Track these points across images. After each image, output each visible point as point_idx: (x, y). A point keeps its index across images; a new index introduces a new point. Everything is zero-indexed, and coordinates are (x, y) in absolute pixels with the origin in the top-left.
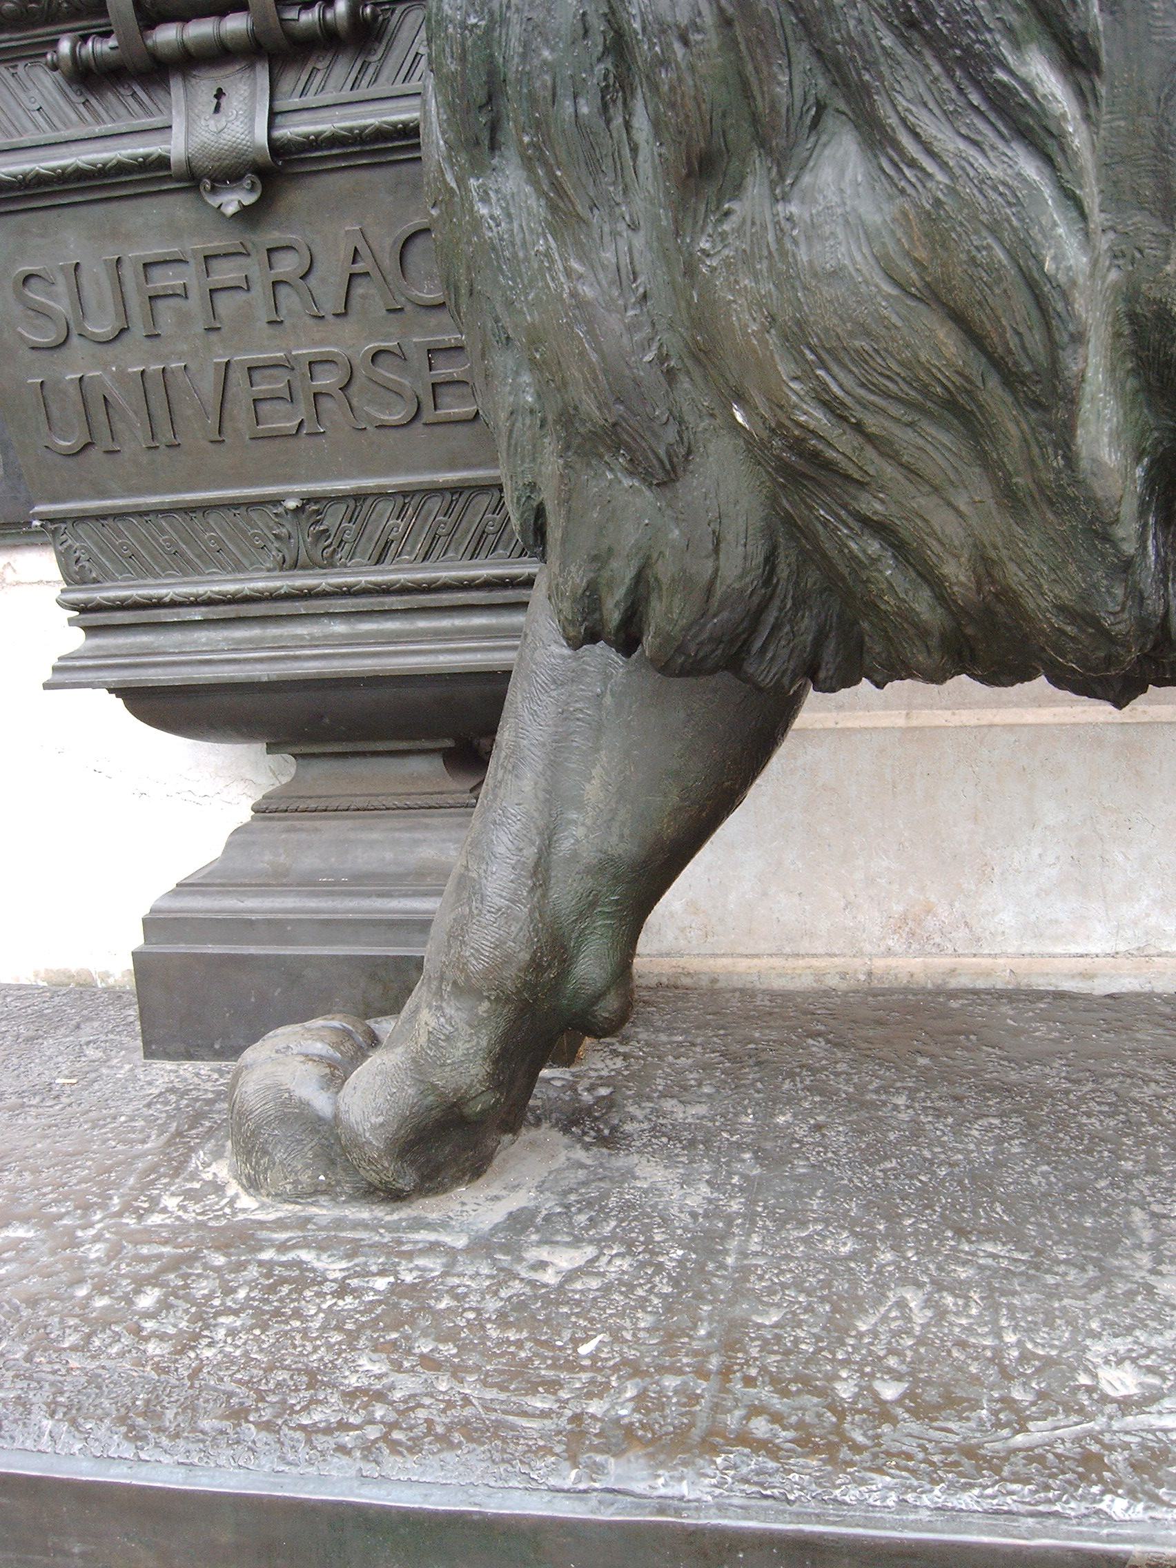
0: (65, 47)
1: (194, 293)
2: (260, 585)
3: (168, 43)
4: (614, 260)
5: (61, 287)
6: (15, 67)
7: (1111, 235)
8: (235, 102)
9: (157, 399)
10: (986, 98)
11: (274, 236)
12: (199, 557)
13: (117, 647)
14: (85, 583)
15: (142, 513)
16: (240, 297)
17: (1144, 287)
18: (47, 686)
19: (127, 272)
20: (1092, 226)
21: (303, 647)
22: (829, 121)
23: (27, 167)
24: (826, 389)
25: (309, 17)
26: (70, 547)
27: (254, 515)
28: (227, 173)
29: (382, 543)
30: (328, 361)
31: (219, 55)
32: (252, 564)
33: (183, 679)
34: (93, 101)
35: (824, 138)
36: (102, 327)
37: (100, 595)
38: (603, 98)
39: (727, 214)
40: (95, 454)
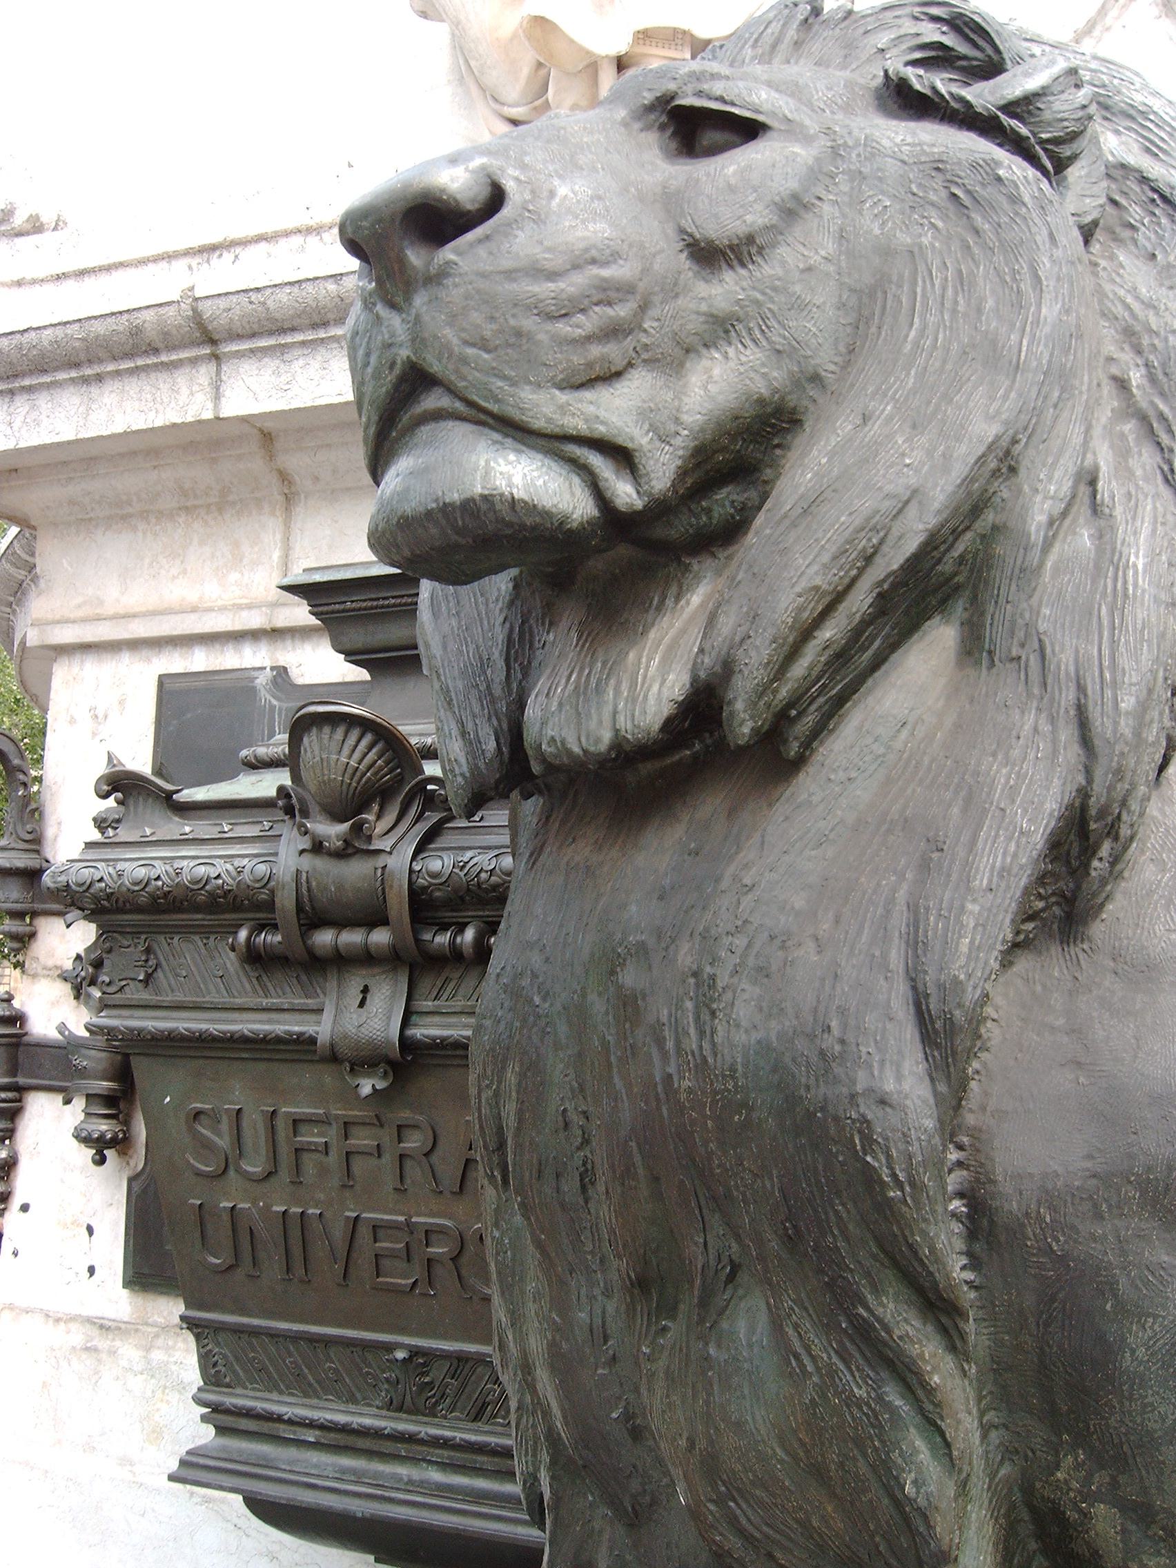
0: (243, 934)
1: (333, 1152)
2: (367, 1421)
3: (324, 946)
4: (588, 1321)
5: (224, 1126)
6: (208, 938)
7: (1002, 1431)
8: (377, 1001)
9: (295, 1233)
10: (851, 1322)
11: (405, 1115)
12: (318, 1382)
13: (240, 1452)
14: (218, 1386)
15: (274, 1335)
16: (373, 1161)
17: (1038, 1485)
18: (172, 1478)
19: (280, 1124)
20: (955, 1453)
21: (398, 1489)
22: (743, 1277)
23: (204, 1026)
24: (736, 1518)
25: (443, 939)
26: (211, 1351)
27: (369, 1356)
28: (365, 1059)
29: (480, 1403)
30: (442, 1230)
31: (367, 958)
32: (364, 1399)
33: (288, 1499)
34: (265, 978)
35: (741, 1292)
36: (254, 1167)
37: (229, 1401)
38: (581, 1180)
39: (665, 1329)
40: (240, 1274)
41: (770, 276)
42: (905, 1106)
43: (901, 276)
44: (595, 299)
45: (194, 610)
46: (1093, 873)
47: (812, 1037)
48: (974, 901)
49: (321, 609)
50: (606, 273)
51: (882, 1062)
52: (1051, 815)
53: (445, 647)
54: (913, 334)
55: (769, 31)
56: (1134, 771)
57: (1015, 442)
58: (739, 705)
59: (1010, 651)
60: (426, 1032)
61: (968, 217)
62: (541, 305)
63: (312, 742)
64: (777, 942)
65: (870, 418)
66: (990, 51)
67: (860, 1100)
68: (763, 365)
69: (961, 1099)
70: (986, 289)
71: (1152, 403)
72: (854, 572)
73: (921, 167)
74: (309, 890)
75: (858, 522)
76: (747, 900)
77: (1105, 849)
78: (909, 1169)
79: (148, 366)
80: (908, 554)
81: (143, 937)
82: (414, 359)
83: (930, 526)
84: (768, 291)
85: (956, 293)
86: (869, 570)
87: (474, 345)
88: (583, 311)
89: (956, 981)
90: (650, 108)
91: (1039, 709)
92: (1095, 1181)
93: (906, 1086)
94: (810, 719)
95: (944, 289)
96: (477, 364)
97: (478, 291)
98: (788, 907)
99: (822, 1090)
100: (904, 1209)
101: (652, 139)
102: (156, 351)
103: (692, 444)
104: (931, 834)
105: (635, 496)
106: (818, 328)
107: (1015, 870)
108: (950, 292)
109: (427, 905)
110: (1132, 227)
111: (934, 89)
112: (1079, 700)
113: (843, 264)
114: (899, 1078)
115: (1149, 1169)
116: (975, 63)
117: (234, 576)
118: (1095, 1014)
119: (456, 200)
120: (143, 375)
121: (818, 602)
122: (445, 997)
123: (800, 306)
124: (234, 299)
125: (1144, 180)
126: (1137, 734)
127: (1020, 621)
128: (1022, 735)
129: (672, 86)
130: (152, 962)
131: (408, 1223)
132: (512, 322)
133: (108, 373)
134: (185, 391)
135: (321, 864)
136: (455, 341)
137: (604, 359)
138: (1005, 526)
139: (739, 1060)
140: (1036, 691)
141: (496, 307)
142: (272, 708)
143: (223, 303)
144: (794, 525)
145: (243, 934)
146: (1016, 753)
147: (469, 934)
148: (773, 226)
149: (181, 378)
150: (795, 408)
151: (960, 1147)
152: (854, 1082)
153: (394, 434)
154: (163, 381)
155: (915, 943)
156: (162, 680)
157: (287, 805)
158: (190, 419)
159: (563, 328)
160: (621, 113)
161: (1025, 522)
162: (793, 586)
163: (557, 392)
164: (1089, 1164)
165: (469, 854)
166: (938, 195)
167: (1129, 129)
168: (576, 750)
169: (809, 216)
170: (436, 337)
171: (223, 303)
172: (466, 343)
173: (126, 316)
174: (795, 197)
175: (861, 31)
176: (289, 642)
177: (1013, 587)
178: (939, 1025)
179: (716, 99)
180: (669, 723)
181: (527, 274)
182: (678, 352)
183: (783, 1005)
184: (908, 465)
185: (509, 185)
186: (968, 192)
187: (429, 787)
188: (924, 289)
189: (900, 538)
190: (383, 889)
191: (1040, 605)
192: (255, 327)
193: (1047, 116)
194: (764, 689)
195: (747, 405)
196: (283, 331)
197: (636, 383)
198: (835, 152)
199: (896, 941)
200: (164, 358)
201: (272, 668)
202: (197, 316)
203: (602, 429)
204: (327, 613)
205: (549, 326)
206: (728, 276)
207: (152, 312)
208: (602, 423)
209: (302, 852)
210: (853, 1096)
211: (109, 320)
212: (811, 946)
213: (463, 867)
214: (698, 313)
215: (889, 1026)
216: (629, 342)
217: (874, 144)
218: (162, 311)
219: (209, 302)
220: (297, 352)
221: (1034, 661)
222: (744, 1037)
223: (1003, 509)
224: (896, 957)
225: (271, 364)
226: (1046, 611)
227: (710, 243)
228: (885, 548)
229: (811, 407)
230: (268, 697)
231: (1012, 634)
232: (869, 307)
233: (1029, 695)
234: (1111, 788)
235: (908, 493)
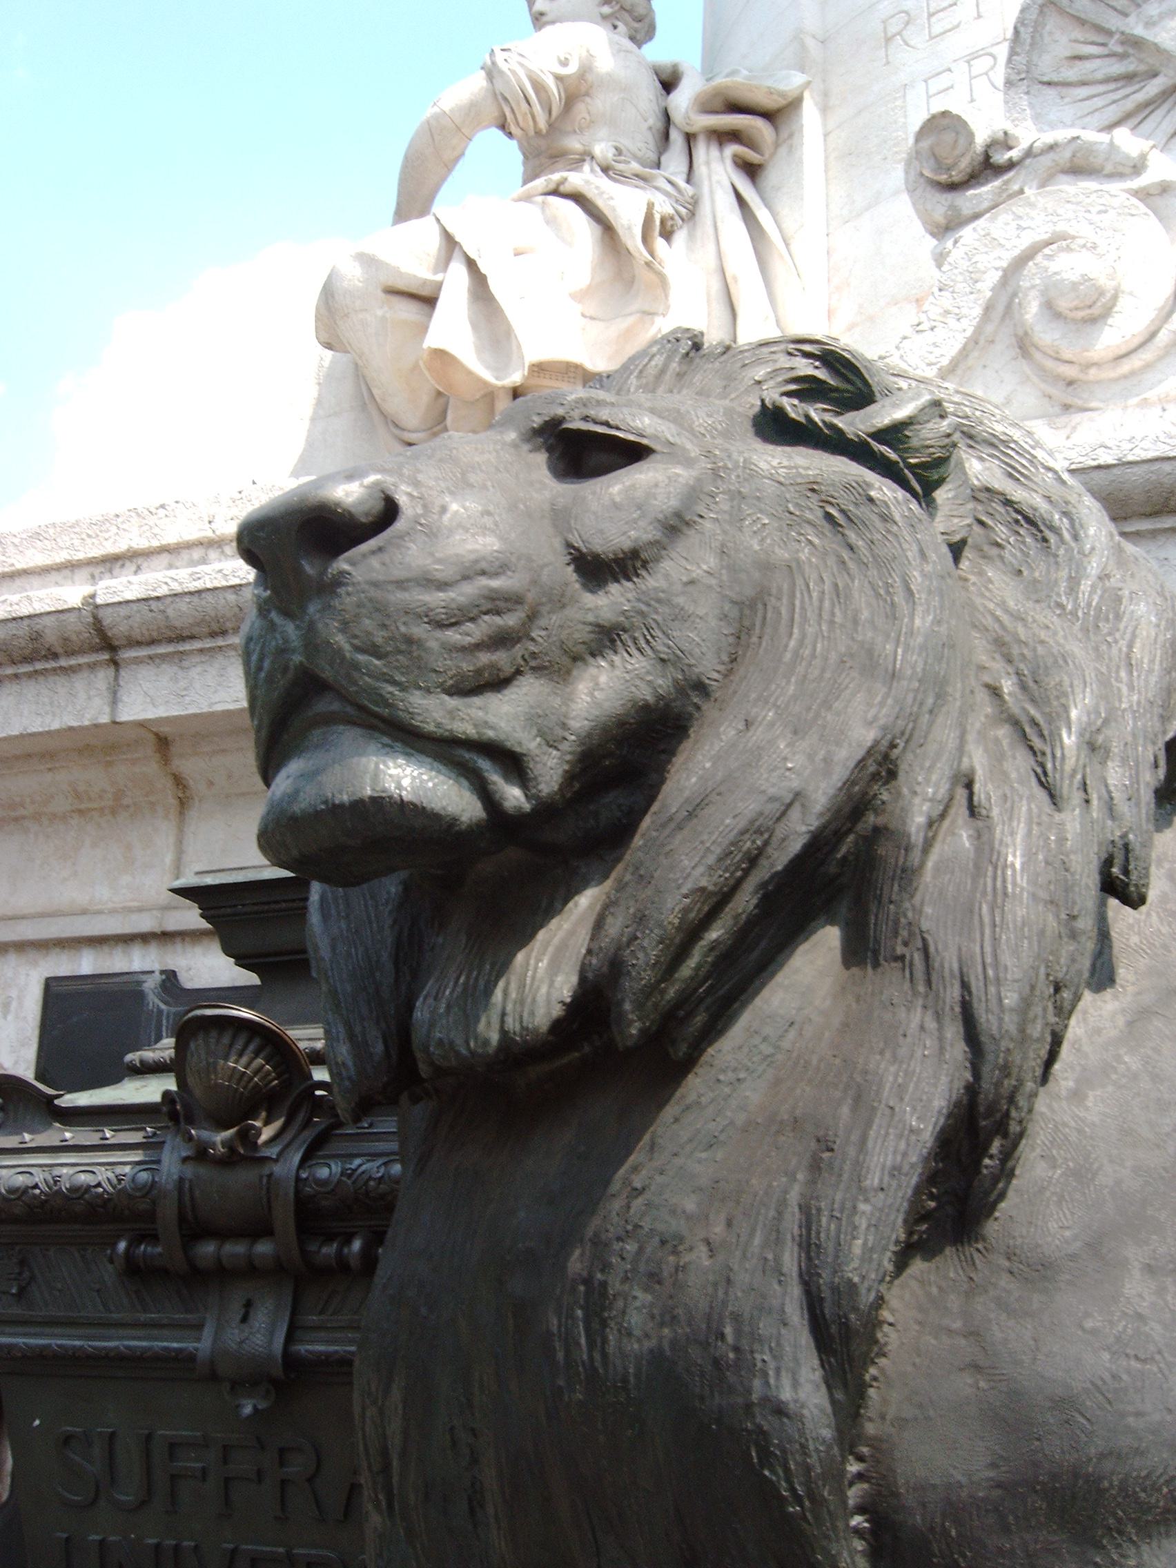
0: (122, 1246)
8: (260, 1319)
25: (330, 1250)
36: (126, 1498)
41: (655, 589)
42: (802, 1416)
43: (780, 589)
44: (484, 609)
45: (84, 912)
46: (985, 1171)
47: (705, 1345)
48: (866, 1200)
49: (212, 912)
50: (495, 583)
51: (778, 1371)
52: (939, 1112)
53: (333, 948)
54: (792, 643)
55: (653, 363)
56: (1021, 1067)
57: (893, 746)
58: (627, 1006)
59: (894, 950)
60: (310, 1347)
63: (197, 1046)
64: (669, 1247)
65: (752, 724)
66: (859, 384)
67: (757, 1410)
68: (648, 673)
69: (859, 1407)
70: (862, 600)
71: (1024, 709)
72: (739, 874)
73: (797, 488)
74: (192, 1198)
75: (742, 823)
76: (638, 1203)
77: (996, 1146)
78: (808, 1483)
79: (46, 670)
80: (791, 855)
81: (18, 1248)
83: (812, 828)
84: (653, 603)
85: (833, 605)
88: (472, 620)
89: (852, 1286)
90: (538, 432)
91: (925, 1007)
92: (998, 1493)
93: (802, 1395)
94: (700, 1019)
95: (821, 601)
96: (368, 670)
97: (371, 600)
99: (717, 1399)
100: (805, 1525)
102: (55, 656)
103: (579, 749)
105: (523, 799)
107: (906, 1168)
108: (827, 604)
109: (316, 1214)
110: (998, 545)
111: (807, 417)
112: (963, 997)
113: (725, 578)
114: (796, 1384)
115: (1054, 1477)
117: (126, 879)
118: (992, 1316)
119: (349, 513)
120: (41, 679)
121: (703, 903)
123: (681, 616)
124: (135, 607)
125: (1008, 503)
126: (1022, 1030)
127: (903, 920)
129: (560, 411)
130: (26, 1274)
131: (289, 1555)
132: (403, 629)
133: (7, 676)
134: (82, 695)
135: (203, 1171)
136: (347, 647)
137: (492, 666)
138: (886, 828)
139: (631, 1371)
140: (921, 988)
142: (160, 1012)
143: (123, 611)
144: (680, 828)
145: (122, 1246)
146: (903, 1052)
147: (357, 1245)
148: (657, 542)
149: (79, 683)
151: (860, 1459)
152: (749, 1391)
153: (286, 737)
154: (61, 685)
155: (809, 1247)
156: (50, 984)
157: (169, 1112)
158: (87, 723)
159: (453, 636)
160: (512, 435)
161: (904, 823)
162: (679, 888)
163: (446, 698)
164: (991, 1474)
165: (357, 1162)
166: (816, 515)
167: (992, 456)
168: (464, 1051)
169: (692, 532)
171: (123, 611)
172: (358, 649)
173: (26, 622)
174: (678, 515)
175: (740, 365)
176: (179, 946)
177: (896, 888)
178: (834, 1329)
180: (557, 1026)
181: (419, 585)
182: (566, 660)
183: (676, 1311)
184: (789, 769)
185: (402, 500)
186: (842, 511)
187: (318, 1093)
188: (802, 602)
189: (784, 840)
190: (269, 1201)
191: (922, 903)
192: (155, 634)
193: (915, 442)
194: (652, 989)
195: (633, 711)
196: (182, 638)
197: (524, 690)
198: (716, 474)
199: (789, 1243)
200: (63, 662)
201: (162, 972)
202: (98, 625)
203: (491, 734)
204: (219, 916)
205: (438, 634)
206: (614, 588)
207: (53, 618)
208: (492, 728)
209: (185, 1160)
210: (749, 1407)
211: (10, 625)
212: (703, 1249)
214: (584, 623)
215: (783, 1331)
216: (518, 650)
218: (62, 617)
219: (110, 610)
220: (196, 659)
221: (918, 958)
222: (636, 1346)
223: (884, 811)
224: (790, 1260)
225: (169, 670)
226: (928, 910)
227: (596, 557)
228: (769, 850)
230: (157, 1001)
231: (896, 933)
232: (750, 617)
233: (915, 993)
234: (998, 1084)
235: (791, 796)
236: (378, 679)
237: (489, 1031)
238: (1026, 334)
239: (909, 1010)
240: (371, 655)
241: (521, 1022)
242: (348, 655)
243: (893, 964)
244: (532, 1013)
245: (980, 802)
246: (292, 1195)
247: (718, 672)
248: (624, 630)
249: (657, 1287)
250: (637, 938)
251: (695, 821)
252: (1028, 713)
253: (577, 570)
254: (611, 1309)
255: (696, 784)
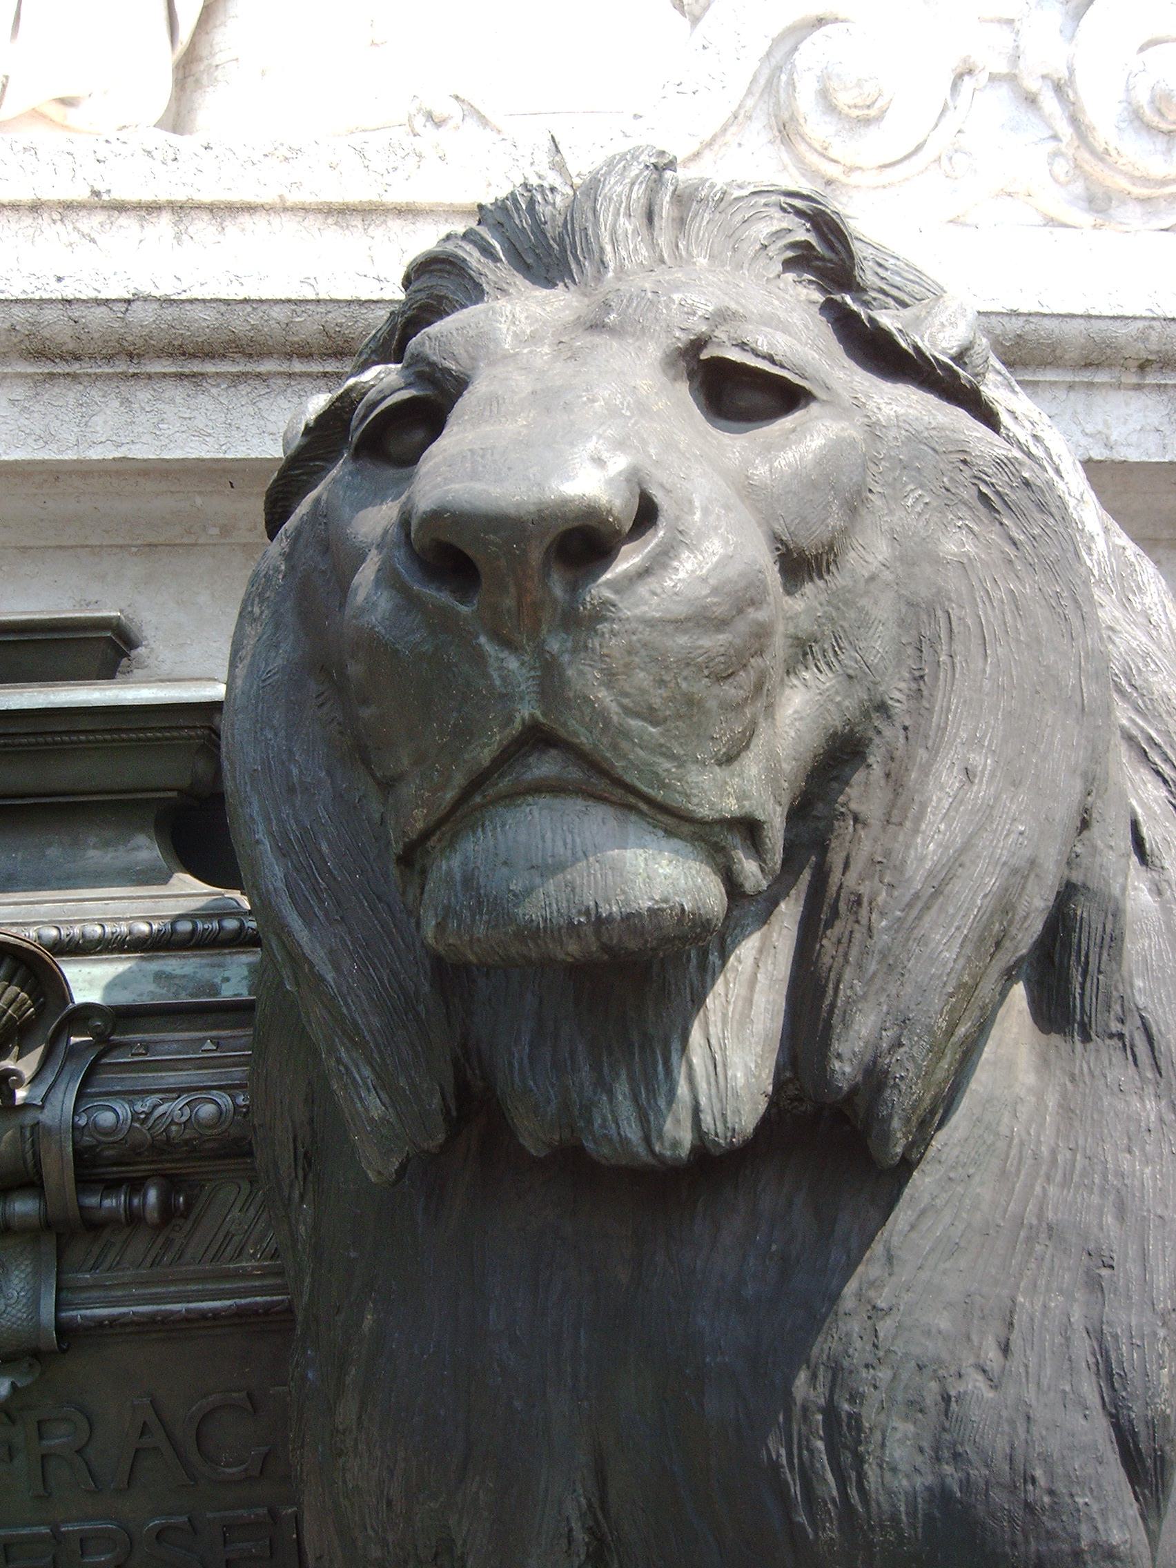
51: (1103, 1512)
53: (337, 968)
58: (896, 1123)
59: (1107, 1025)
60: (88, 1312)
61: (1001, 524)
62: (711, 664)
64: (928, 1372)
65: (975, 776)
68: (837, 693)
76: (885, 1327)
80: (1035, 936)
82: (541, 719)
85: (1015, 619)
86: (998, 956)
87: (637, 715)
91: (1158, 1097)
96: (641, 738)
97: (645, 645)
98: (934, 1330)
101: (683, 389)
104: (1092, 1246)
106: (878, 644)
108: (1009, 618)
113: (899, 571)
116: (829, 265)
122: (106, 1265)
127: (1114, 993)
128: (1152, 1126)
136: (614, 707)
138: (1085, 886)
139: (902, 1509)
140: (1149, 1075)
141: (666, 668)
144: (927, 907)
150: (860, 740)
155: (1107, 1372)
161: (1108, 885)
166: (968, 494)
168: (642, 1150)
170: (586, 699)
172: (627, 711)
177: (1105, 957)
179: (764, 357)
180: (765, 1123)
181: (698, 625)
184: (1021, 833)
186: (997, 493)
188: (986, 613)
189: (1026, 918)
191: (1131, 976)
205: (715, 690)
206: (808, 588)
213: (147, 1118)
217: (907, 427)
222: (905, 1482)
224: (1089, 1389)
226: (1139, 983)
229: (877, 740)
231: (1109, 1008)
233: (1143, 1079)
236: (653, 751)
237: (678, 1134)
238: (793, 118)
239: (1142, 1099)
240: (644, 719)
241: (725, 1122)
242: (615, 718)
243: (1108, 1041)
244: (737, 1112)
245: (1152, 850)
246: (70, 1149)
247: (900, 690)
248: (816, 641)
249: (920, 1415)
250: (901, 1045)
251: (941, 899)
252: (1142, 730)
253: (782, 570)
254: (868, 1442)
255: (935, 852)
